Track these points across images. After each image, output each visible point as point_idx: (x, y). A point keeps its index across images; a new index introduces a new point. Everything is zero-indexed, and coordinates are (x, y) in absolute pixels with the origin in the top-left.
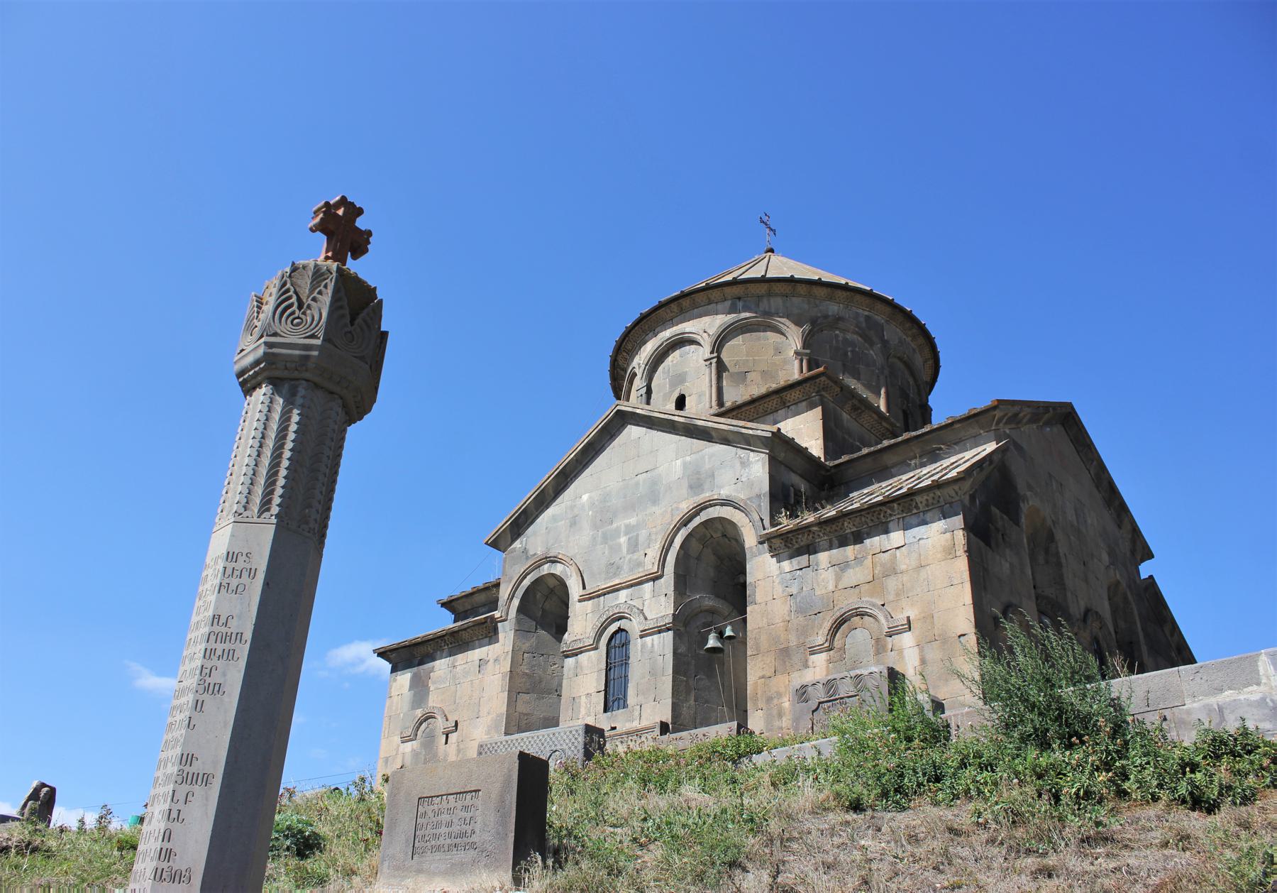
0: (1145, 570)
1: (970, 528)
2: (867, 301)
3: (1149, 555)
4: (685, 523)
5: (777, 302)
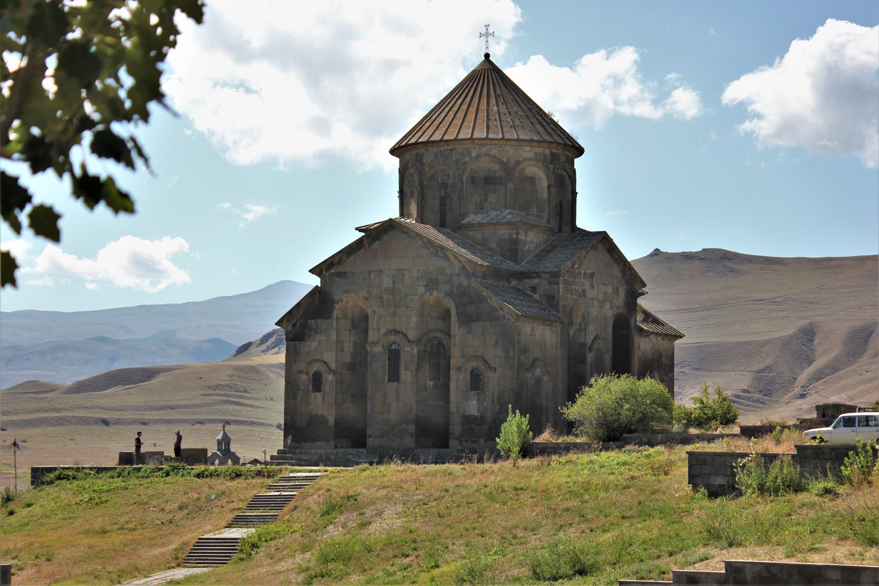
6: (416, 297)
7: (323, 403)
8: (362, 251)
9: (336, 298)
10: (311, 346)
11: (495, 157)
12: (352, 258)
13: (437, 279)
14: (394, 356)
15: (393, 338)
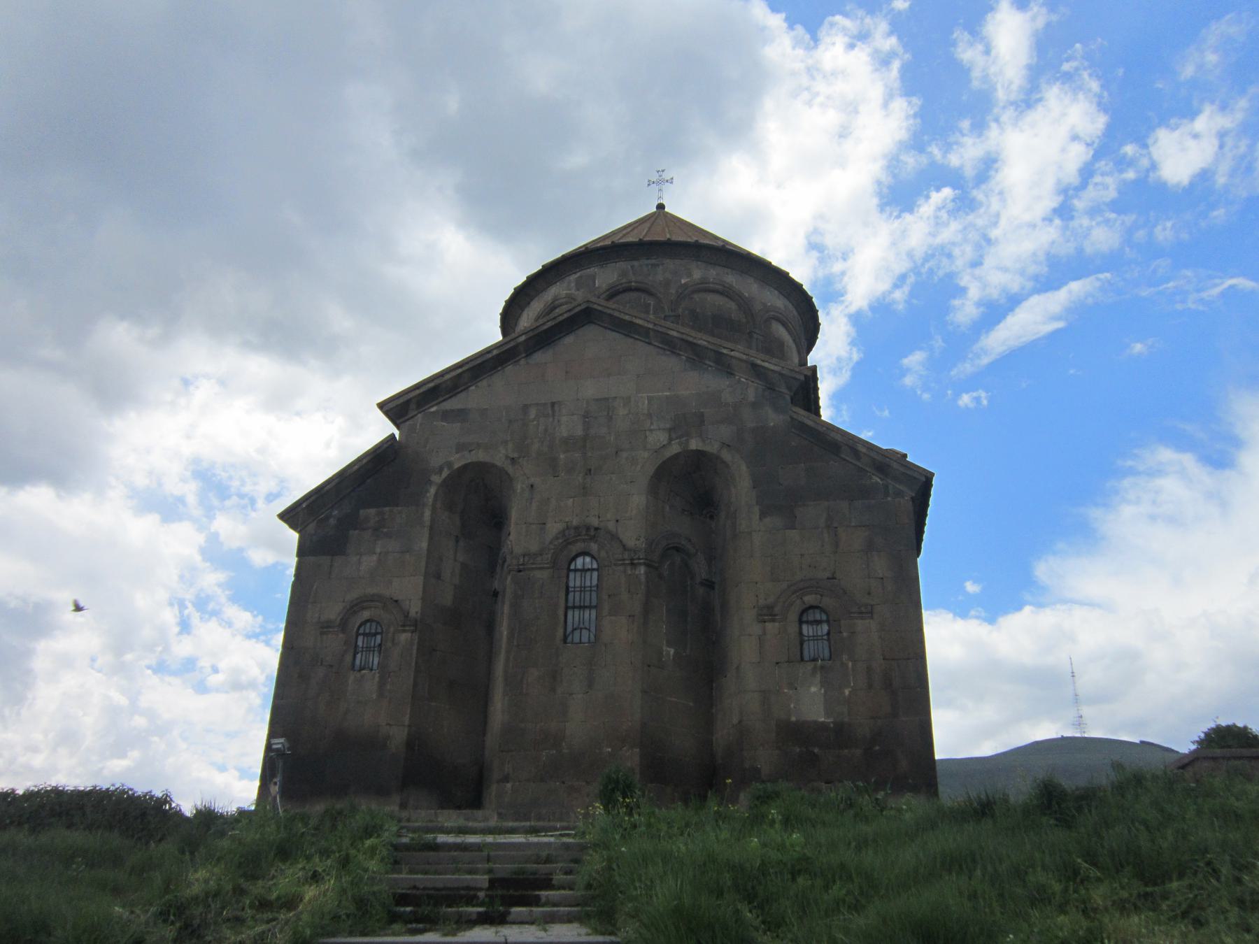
6: (646, 455)
10: (361, 563)
12: (484, 383)
13: (702, 415)
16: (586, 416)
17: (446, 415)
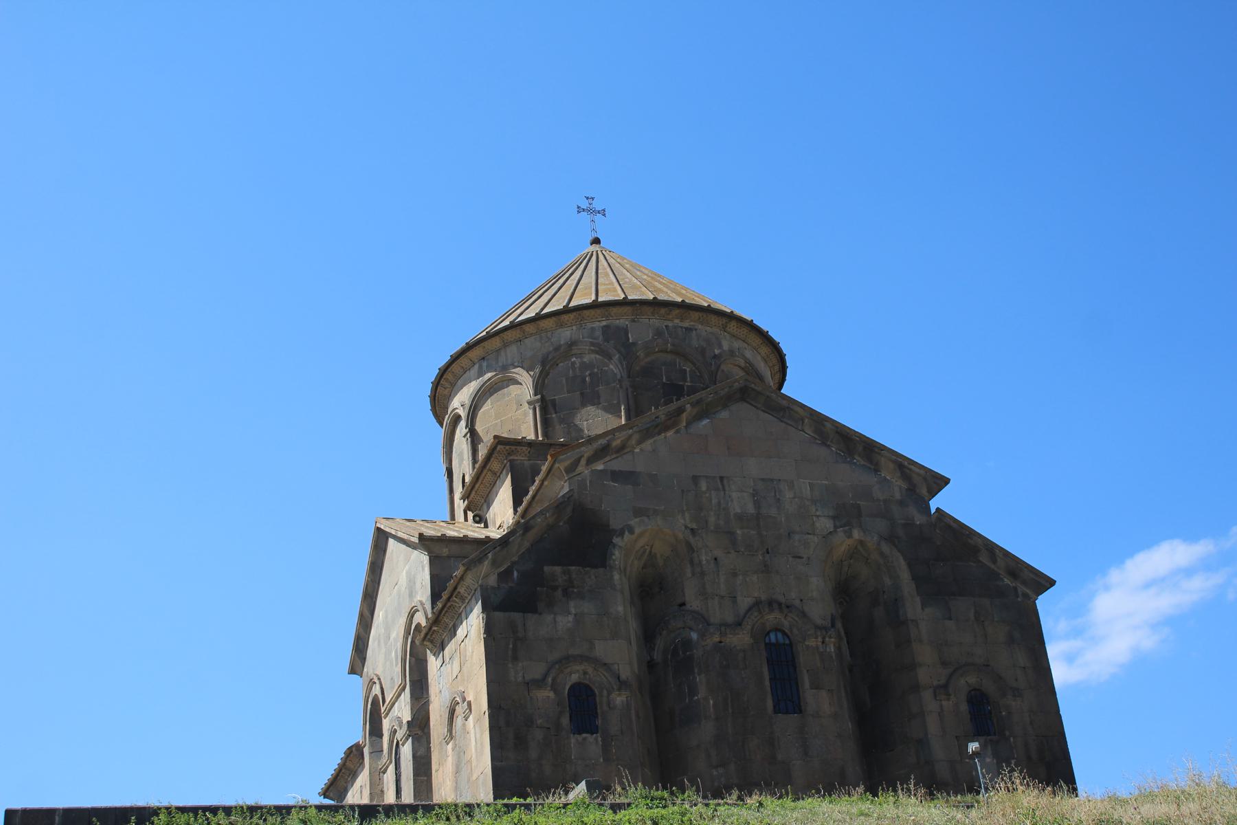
0: (934, 504)
1: (484, 609)
2: (599, 311)
3: (939, 482)
4: (407, 632)
5: (513, 350)
7: (607, 760)
8: (670, 433)
9: (615, 524)
11: (751, 364)
12: (648, 445)
14: (781, 660)
15: (772, 618)
16: (755, 494)
17: (616, 476)
